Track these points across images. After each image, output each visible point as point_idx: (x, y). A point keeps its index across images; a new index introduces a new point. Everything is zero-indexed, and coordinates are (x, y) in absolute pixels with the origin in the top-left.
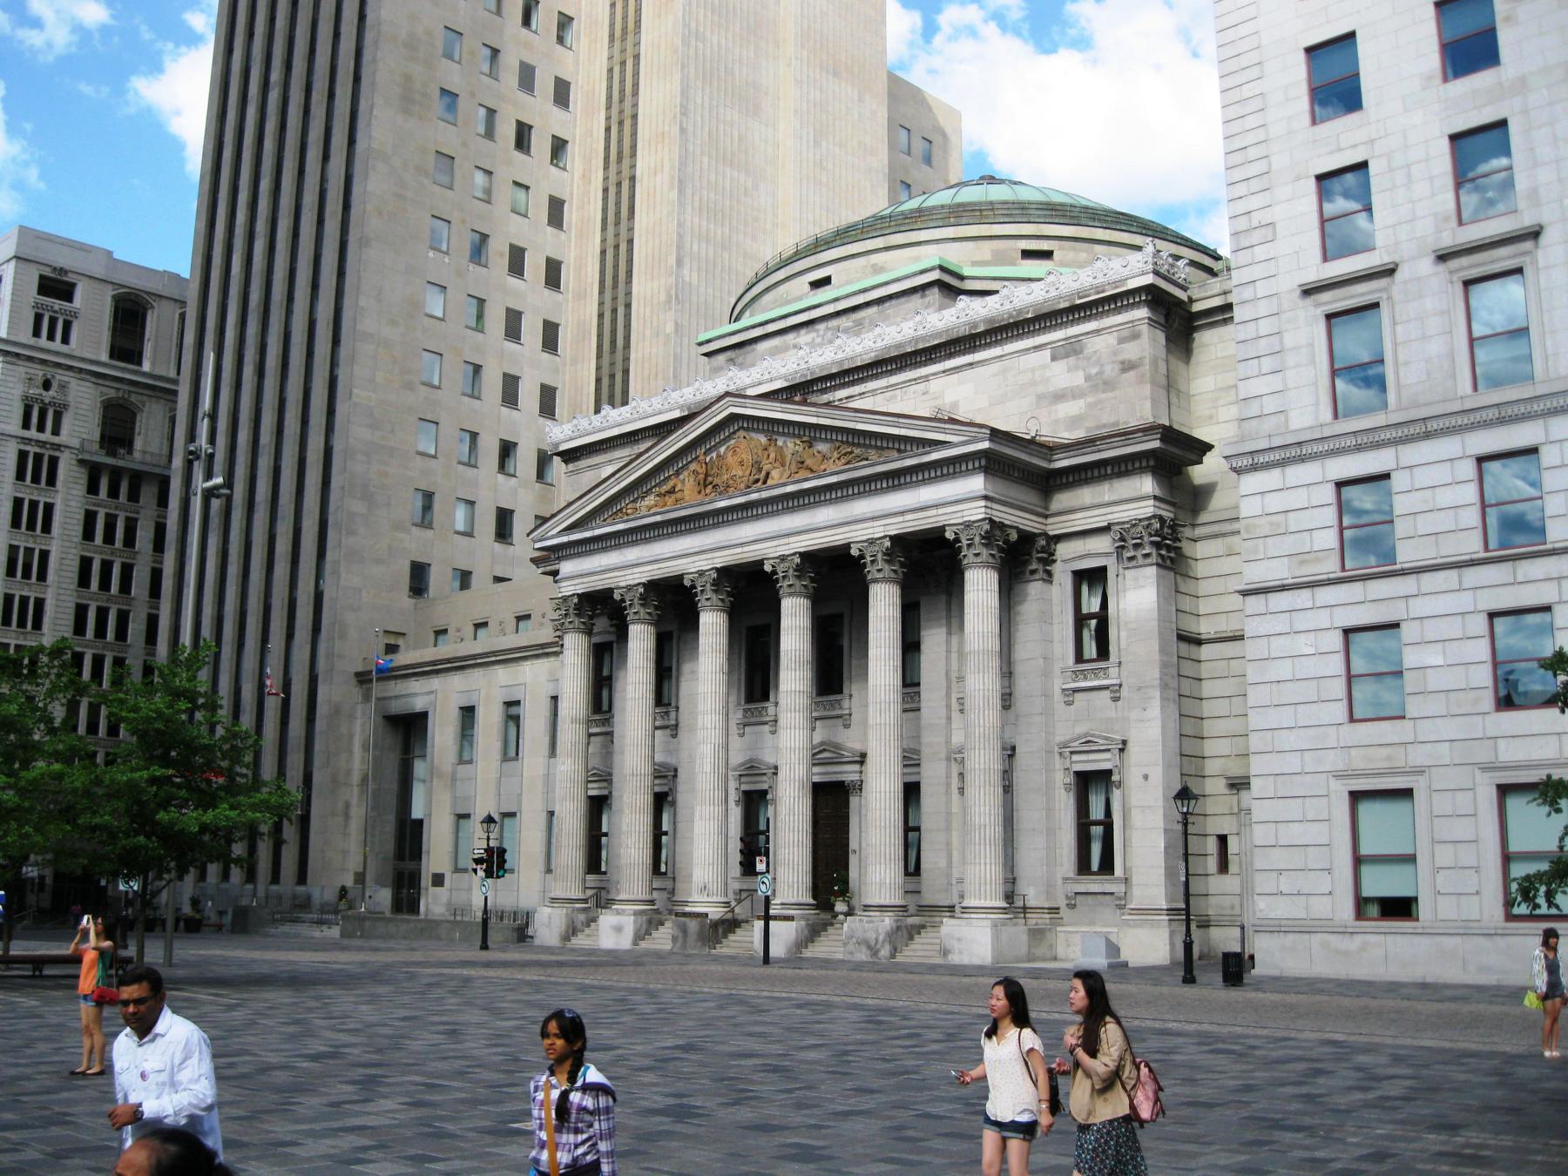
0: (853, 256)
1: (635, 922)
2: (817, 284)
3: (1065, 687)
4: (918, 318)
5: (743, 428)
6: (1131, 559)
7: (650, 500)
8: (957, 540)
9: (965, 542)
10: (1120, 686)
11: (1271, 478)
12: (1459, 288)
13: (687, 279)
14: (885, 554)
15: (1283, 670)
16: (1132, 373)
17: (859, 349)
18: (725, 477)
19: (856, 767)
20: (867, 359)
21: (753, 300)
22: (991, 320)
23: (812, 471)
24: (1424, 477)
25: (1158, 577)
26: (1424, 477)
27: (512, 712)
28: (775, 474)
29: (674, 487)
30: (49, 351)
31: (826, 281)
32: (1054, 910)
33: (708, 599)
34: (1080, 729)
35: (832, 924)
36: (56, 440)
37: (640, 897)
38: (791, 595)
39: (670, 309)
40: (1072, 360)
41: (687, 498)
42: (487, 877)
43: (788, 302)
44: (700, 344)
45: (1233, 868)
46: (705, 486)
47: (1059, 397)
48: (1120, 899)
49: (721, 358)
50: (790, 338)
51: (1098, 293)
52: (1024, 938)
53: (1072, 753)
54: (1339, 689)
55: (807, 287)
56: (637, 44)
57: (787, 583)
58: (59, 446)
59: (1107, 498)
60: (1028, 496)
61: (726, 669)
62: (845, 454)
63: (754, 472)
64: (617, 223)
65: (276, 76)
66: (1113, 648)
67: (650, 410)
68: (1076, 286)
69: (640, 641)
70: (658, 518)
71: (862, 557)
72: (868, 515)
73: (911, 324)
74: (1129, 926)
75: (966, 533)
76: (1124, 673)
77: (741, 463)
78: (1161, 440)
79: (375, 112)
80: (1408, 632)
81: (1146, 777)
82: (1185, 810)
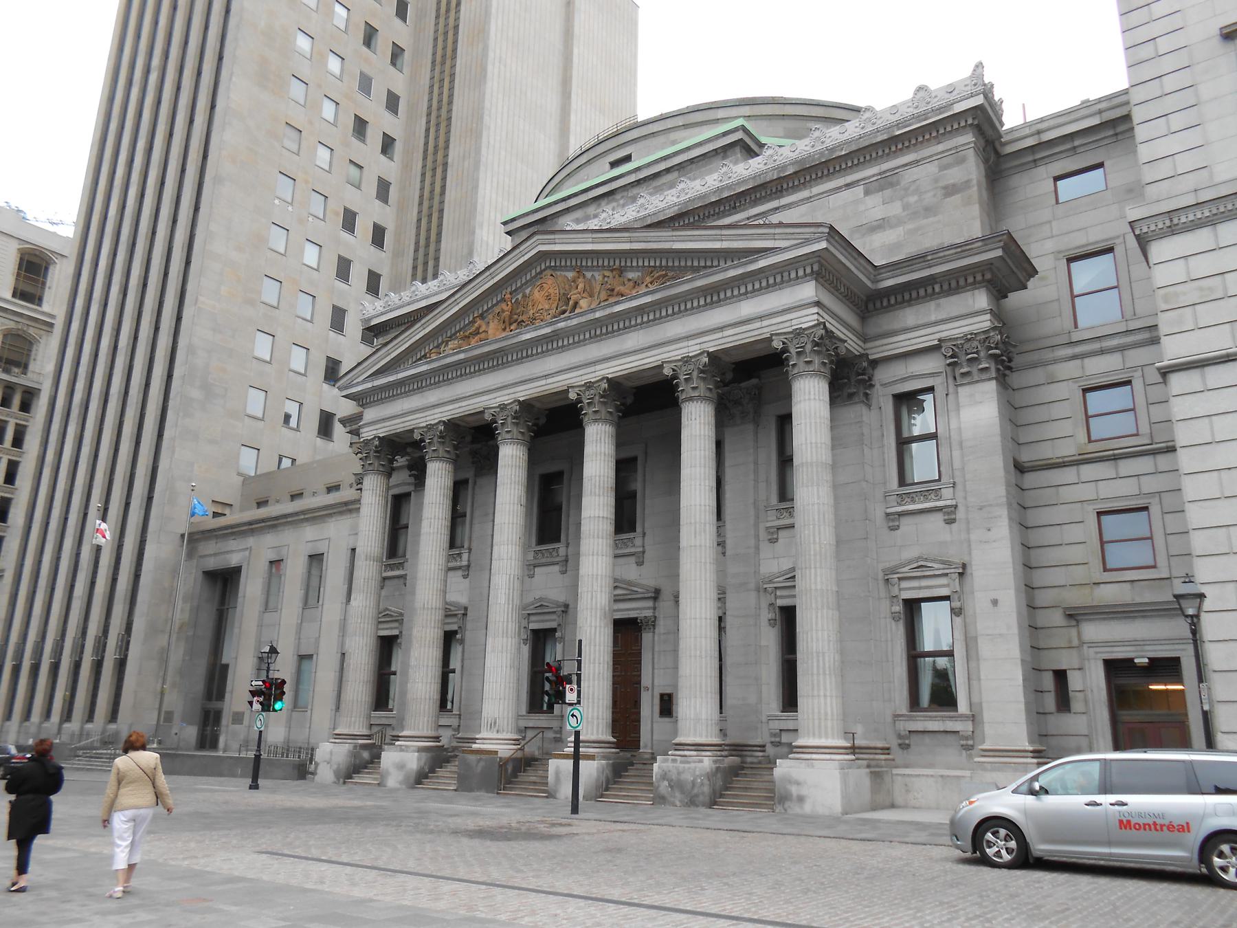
1: (419, 759)
3: (889, 511)
4: (724, 169)
6: (963, 375)
8: (785, 350)
9: (793, 351)
10: (956, 507)
14: (702, 371)
16: (956, 199)
17: (662, 205)
18: (532, 312)
19: (650, 604)
22: (802, 161)
23: (622, 296)
25: (999, 393)
27: (316, 559)
28: (584, 303)
29: (478, 328)
31: (628, 158)
32: (886, 750)
33: (508, 432)
34: (908, 554)
35: (632, 764)
37: (425, 733)
38: (596, 421)
40: (888, 192)
42: (263, 710)
44: (505, 223)
45: (1077, 705)
46: (510, 324)
48: (967, 738)
51: (920, 121)
52: (867, 782)
53: (899, 579)
55: (608, 166)
56: (453, 66)
59: (933, 318)
60: (851, 319)
61: (524, 501)
62: (658, 278)
64: (431, 198)
69: (438, 477)
70: (462, 356)
71: (675, 377)
73: (715, 176)
74: (985, 770)
75: (795, 342)
76: (960, 494)
77: (548, 298)
78: (1003, 248)
81: (995, 602)
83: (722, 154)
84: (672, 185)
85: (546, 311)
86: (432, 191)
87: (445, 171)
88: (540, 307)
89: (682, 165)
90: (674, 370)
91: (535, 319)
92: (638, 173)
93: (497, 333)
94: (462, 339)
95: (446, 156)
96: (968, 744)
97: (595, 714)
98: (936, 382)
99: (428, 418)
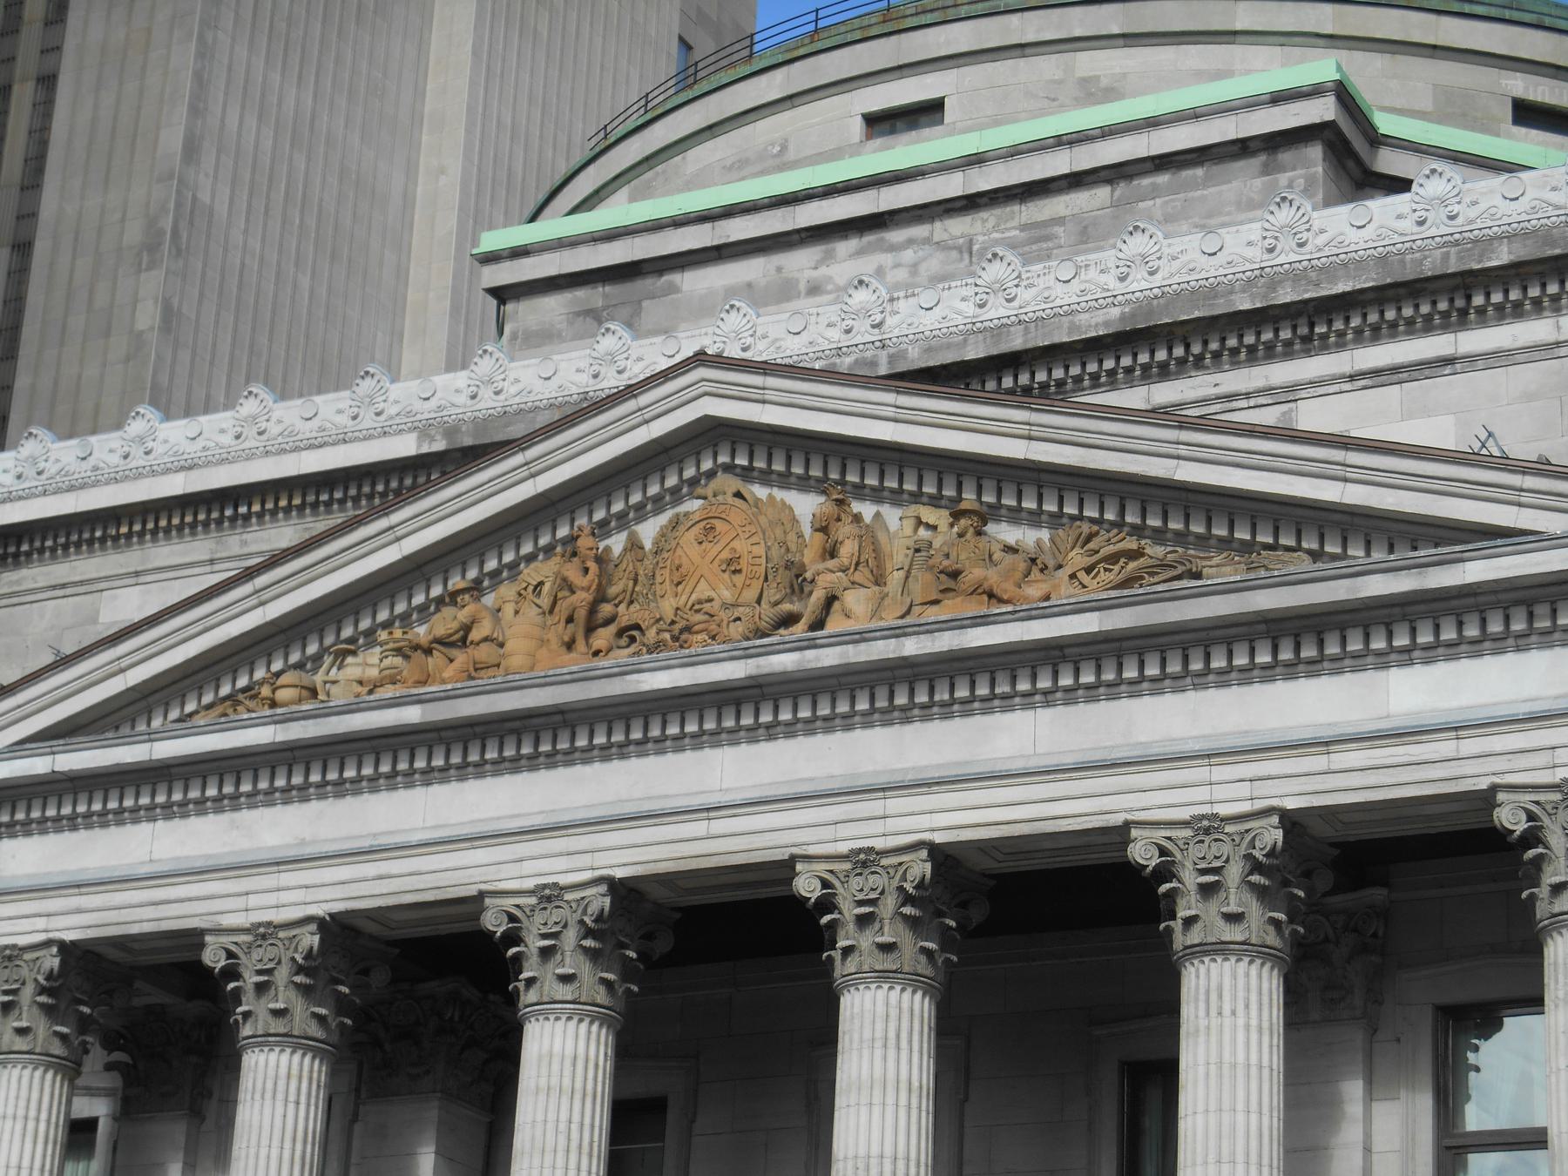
0: (1021, 49)
2: (882, 123)
4: (1284, 215)
5: (729, 468)
7: (368, 664)
13: (205, 197)
17: (1064, 296)
18: (667, 607)
20: (1094, 324)
21: (649, 161)
28: (857, 601)
29: (467, 629)
31: (928, 112)
33: (566, 979)
38: (884, 976)
39: (152, 265)
41: (516, 661)
44: (491, 258)
46: (590, 629)
49: (553, 306)
50: (800, 262)
55: (858, 125)
57: (866, 940)
62: (1113, 559)
63: (772, 594)
67: (308, 430)
70: (412, 715)
71: (1165, 872)
72: (1197, 746)
73: (1253, 231)
77: (732, 566)
83: (1263, 158)
84: (1088, 235)
85: (726, 606)
88: (703, 591)
89: (1128, 169)
90: (1163, 852)
91: (688, 629)
92: (974, 172)
93: (543, 653)
94: (398, 651)
99: (253, 901)
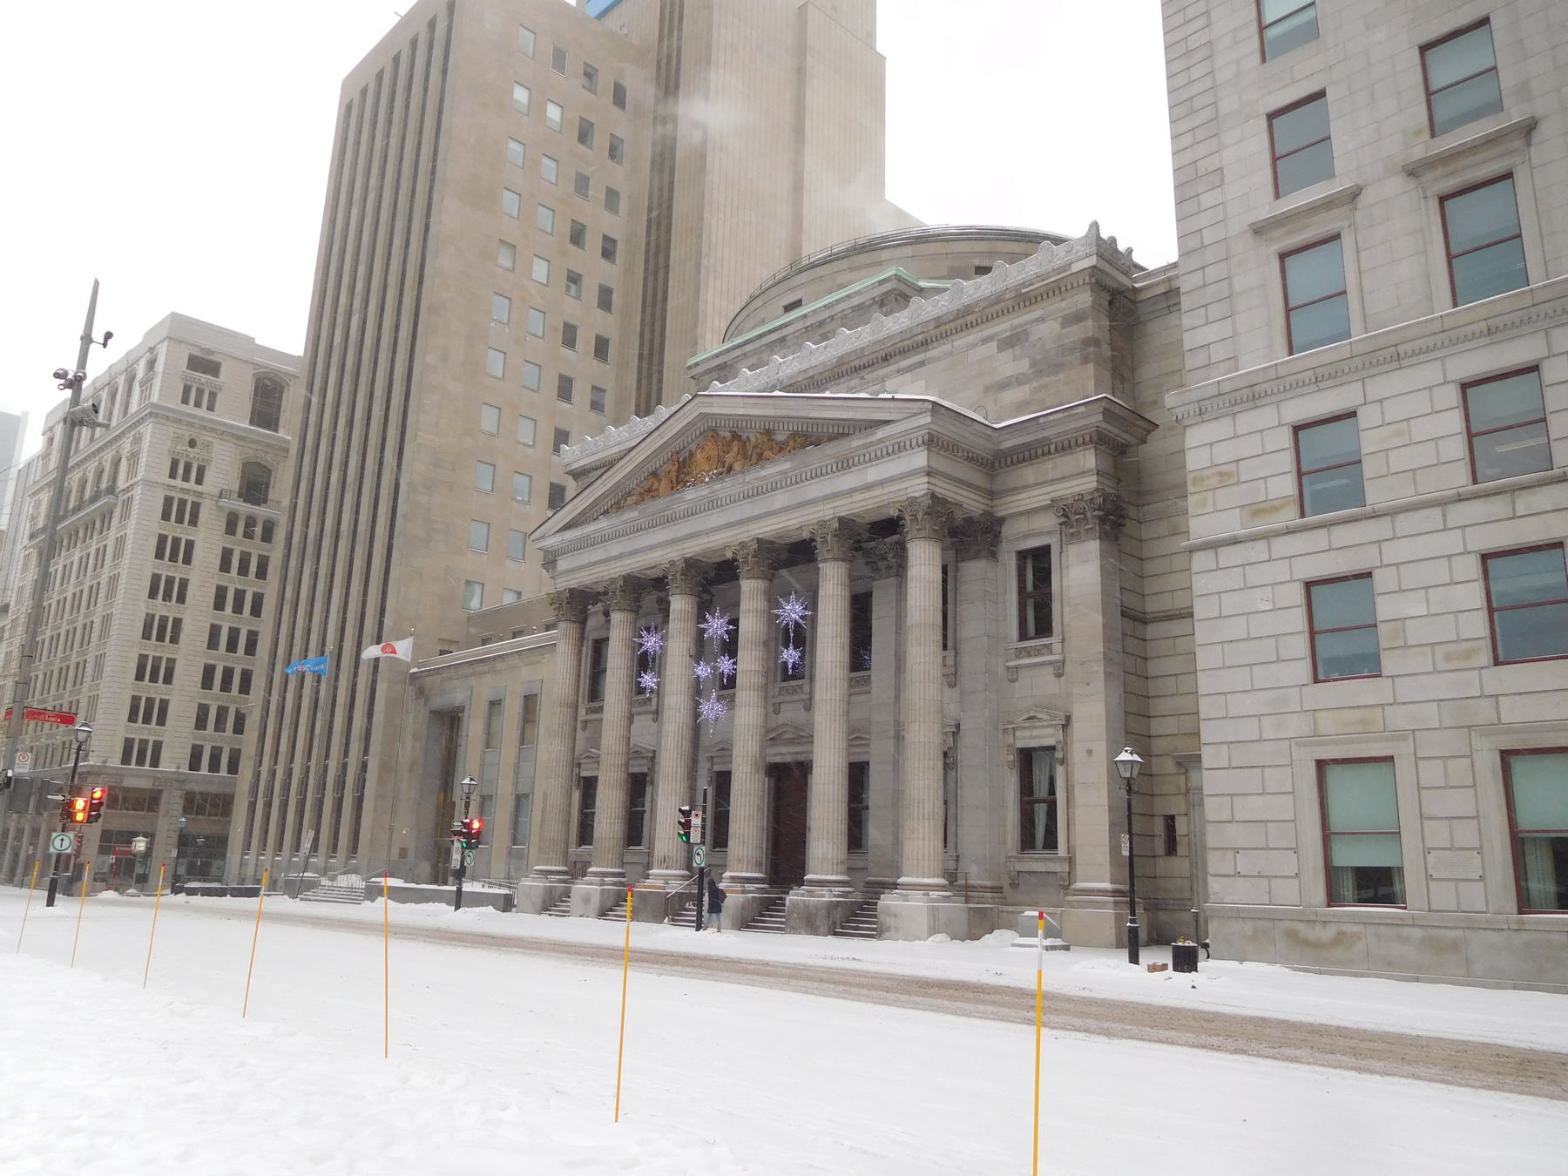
3: (1007, 664)
9: (908, 518)
11: (1221, 428)
12: (1434, 205)
15: (1236, 629)
24: (1395, 411)
25: (1103, 554)
26: (1395, 411)
27: (530, 702)
28: (737, 466)
30: (194, 416)
31: (797, 304)
36: (199, 488)
43: (763, 322)
45: (1181, 850)
47: (1004, 385)
54: (1301, 646)
55: (782, 310)
58: (202, 493)
59: (1050, 477)
64: (654, 304)
65: (373, 182)
66: (1056, 625)
68: (1022, 277)
77: (709, 459)
79: (445, 202)
80: (1381, 580)
81: (1090, 752)
82: (1128, 775)
86: (655, 295)
87: (667, 273)
95: (667, 258)
96: (1065, 883)
97: (745, 853)
98: (1053, 541)
